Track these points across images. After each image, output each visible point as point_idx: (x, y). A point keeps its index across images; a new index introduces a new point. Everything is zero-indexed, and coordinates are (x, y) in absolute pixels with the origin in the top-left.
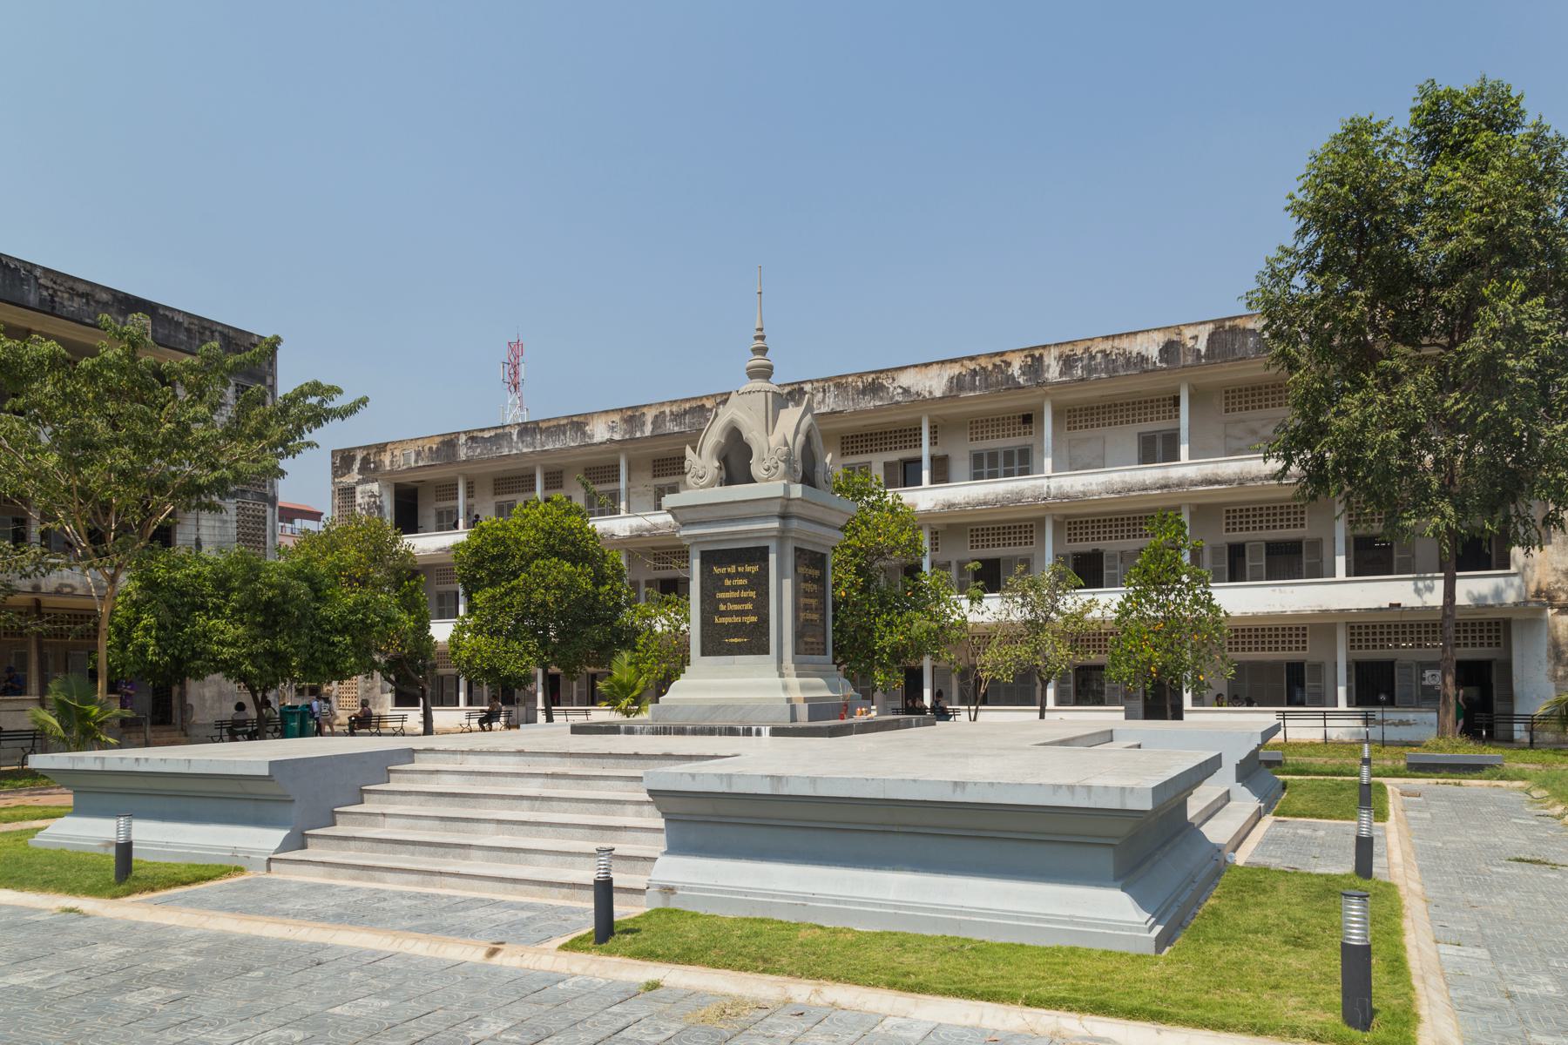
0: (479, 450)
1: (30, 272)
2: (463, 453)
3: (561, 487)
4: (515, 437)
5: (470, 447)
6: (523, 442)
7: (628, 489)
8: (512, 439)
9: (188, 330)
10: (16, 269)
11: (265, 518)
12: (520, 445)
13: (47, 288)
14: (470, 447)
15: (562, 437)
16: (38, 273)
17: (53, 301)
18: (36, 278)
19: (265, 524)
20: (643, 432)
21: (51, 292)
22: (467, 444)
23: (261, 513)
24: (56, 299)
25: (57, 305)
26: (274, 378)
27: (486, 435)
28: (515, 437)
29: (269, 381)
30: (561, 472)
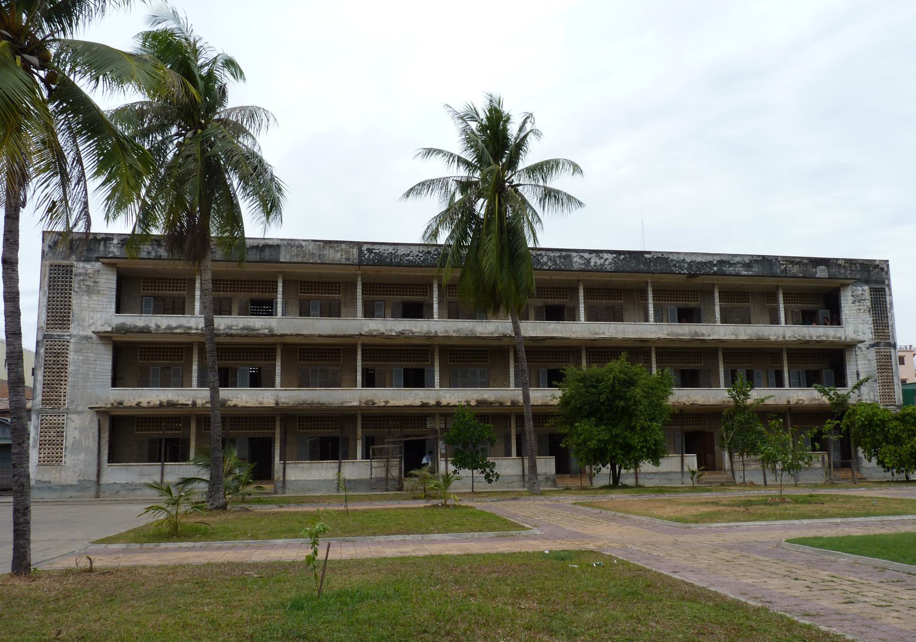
1: (777, 259)
9: (844, 267)
10: (771, 260)
11: (891, 356)
13: (783, 264)
16: (779, 259)
17: (786, 270)
18: (779, 262)
19: (891, 359)
21: (785, 266)
23: (889, 354)
24: (787, 269)
25: (788, 272)
26: (889, 279)
29: (886, 282)
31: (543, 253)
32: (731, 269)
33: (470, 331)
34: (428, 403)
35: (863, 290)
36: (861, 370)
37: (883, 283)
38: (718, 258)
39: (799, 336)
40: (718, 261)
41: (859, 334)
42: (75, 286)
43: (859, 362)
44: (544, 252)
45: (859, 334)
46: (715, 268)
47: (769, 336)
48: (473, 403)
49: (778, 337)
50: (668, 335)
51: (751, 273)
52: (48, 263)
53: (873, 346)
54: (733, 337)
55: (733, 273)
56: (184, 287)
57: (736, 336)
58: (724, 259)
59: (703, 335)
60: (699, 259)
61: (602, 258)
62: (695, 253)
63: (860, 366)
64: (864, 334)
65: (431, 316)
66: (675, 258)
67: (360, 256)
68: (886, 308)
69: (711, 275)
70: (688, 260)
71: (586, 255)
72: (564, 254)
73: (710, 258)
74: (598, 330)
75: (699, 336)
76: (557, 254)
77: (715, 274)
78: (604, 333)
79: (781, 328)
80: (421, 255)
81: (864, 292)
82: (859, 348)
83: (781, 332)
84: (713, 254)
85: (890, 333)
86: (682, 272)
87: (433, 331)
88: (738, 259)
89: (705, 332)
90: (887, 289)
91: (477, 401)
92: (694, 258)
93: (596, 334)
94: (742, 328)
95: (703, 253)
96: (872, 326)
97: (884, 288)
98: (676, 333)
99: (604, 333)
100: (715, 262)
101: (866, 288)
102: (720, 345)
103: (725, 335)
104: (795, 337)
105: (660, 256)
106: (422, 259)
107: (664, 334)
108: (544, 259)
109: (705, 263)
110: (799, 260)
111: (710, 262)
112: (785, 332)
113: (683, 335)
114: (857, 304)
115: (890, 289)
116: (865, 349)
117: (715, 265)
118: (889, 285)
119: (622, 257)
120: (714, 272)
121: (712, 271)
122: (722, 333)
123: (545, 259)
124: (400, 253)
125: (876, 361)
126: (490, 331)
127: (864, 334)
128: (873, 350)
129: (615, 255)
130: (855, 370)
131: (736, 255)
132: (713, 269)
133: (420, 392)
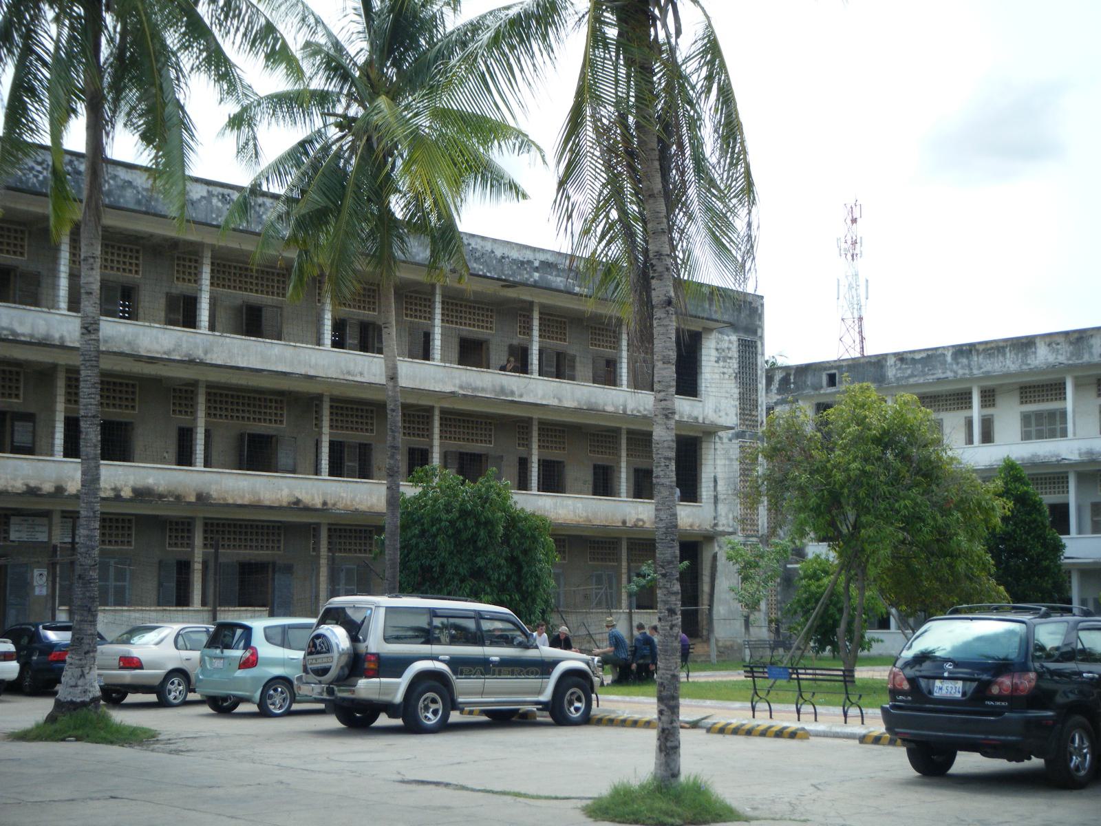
0: (909, 372)
2: (891, 373)
3: (994, 405)
4: (949, 359)
5: (900, 369)
6: (958, 364)
7: (1074, 411)
8: (946, 361)
12: (954, 366)
14: (900, 369)
15: (1001, 358)
20: (1091, 354)
22: (895, 365)
27: (918, 356)
28: (949, 359)
30: (993, 391)
31: (268, 201)
32: (559, 279)
33: (129, 343)
34: (39, 489)
35: (730, 342)
36: (720, 476)
37: (755, 332)
38: (542, 257)
39: (645, 410)
40: (542, 262)
43: (718, 462)
44: (271, 200)
46: (536, 275)
48: (127, 493)
49: (617, 407)
50: (461, 387)
54: (555, 402)
55: (562, 287)
56: (118, 269)
57: (560, 400)
58: (551, 259)
59: (512, 393)
60: (515, 254)
62: (508, 243)
63: (719, 469)
65: (53, 305)
66: (478, 247)
68: (756, 375)
70: (499, 253)
73: (529, 256)
74: (352, 367)
75: (506, 395)
77: (535, 285)
78: (361, 374)
79: (621, 393)
80: (39, 168)
83: (621, 401)
84: (534, 250)
86: (488, 274)
87: (57, 336)
89: (515, 389)
90: (759, 344)
91: (135, 490)
92: (507, 251)
93: (349, 373)
94: (568, 387)
95: (521, 245)
96: (737, 403)
98: (473, 385)
100: (537, 264)
101: (734, 338)
102: (536, 415)
103: (543, 397)
104: (639, 411)
106: (41, 177)
107: (455, 386)
108: (269, 214)
109: (522, 263)
111: (529, 262)
113: (483, 390)
114: (721, 364)
115: (763, 345)
117: (537, 269)
118: (761, 338)
120: (535, 281)
122: (540, 393)
126: (165, 349)
127: (727, 414)
130: (712, 475)
132: (531, 276)
133: (25, 464)
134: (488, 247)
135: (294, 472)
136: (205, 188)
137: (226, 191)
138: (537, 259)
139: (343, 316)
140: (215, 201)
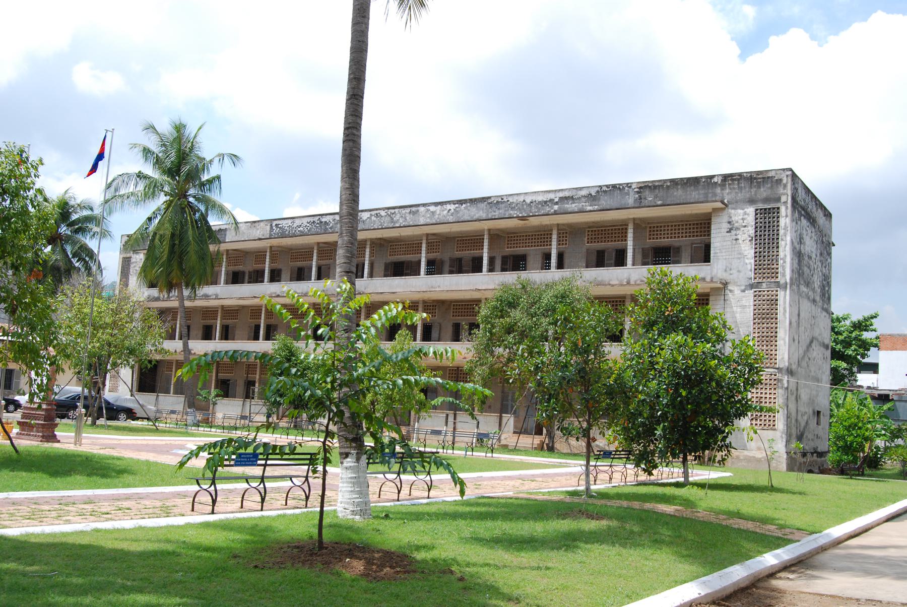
31: (396, 210)
32: (573, 205)
35: (745, 214)
38: (561, 195)
40: (561, 198)
41: (731, 272)
42: (131, 270)
45: (731, 272)
46: (556, 207)
47: (611, 280)
51: (596, 207)
52: (122, 256)
53: (751, 286)
58: (567, 194)
60: (540, 198)
61: (446, 209)
64: (739, 271)
66: (515, 201)
67: (271, 231)
69: (552, 214)
71: (432, 208)
72: (414, 209)
76: (408, 210)
77: (556, 213)
78: (439, 286)
81: (746, 216)
82: (731, 291)
83: (626, 275)
84: (555, 191)
85: (780, 270)
88: (584, 193)
92: (534, 198)
93: (432, 287)
97: (778, 208)
99: (439, 286)
100: (556, 200)
105: (500, 200)
109: (546, 202)
110: (660, 184)
111: (551, 200)
112: (630, 275)
116: (739, 292)
117: (557, 203)
119: (464, 205)
120: (555, 211)
121: (552, 211)
123: (398, 217)
124: (295, 225)
125: (752, 308)
127: (739, 271)
128: (750, 293)
129: (457, 205)
131: (581, 189)
134: (521, 199)
135: (439, 341)
136: (369, 213)
137: (378, 212)
138: (556, 197)
139: (561, 250)
140: (373, 218)
